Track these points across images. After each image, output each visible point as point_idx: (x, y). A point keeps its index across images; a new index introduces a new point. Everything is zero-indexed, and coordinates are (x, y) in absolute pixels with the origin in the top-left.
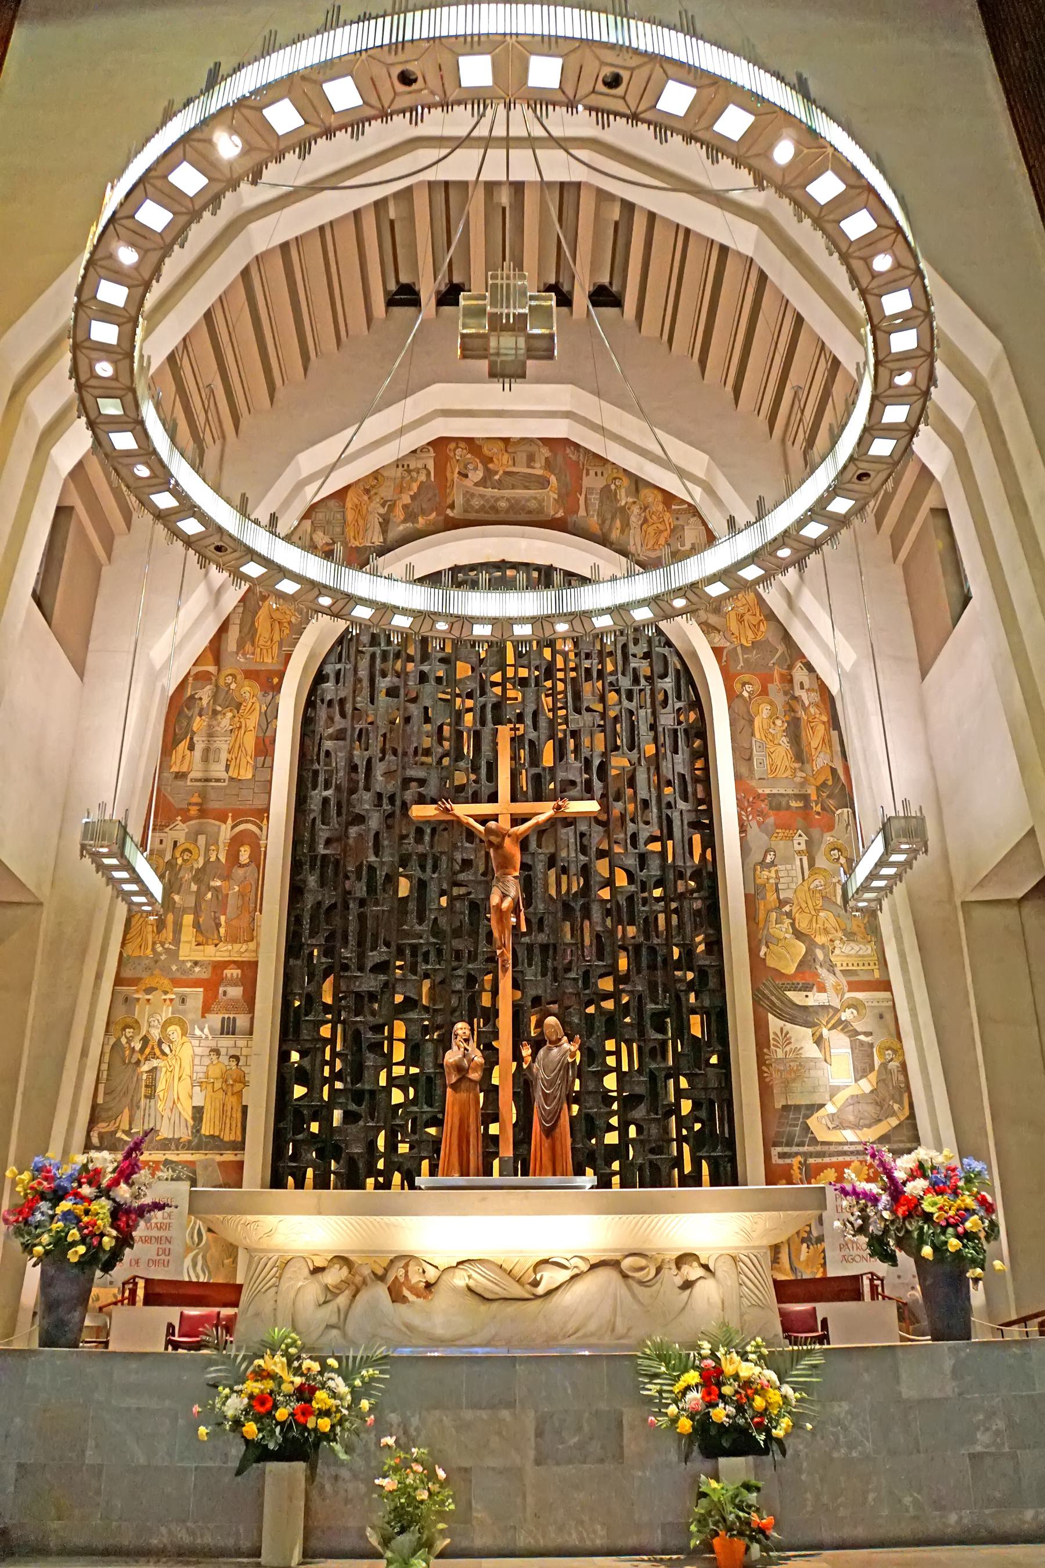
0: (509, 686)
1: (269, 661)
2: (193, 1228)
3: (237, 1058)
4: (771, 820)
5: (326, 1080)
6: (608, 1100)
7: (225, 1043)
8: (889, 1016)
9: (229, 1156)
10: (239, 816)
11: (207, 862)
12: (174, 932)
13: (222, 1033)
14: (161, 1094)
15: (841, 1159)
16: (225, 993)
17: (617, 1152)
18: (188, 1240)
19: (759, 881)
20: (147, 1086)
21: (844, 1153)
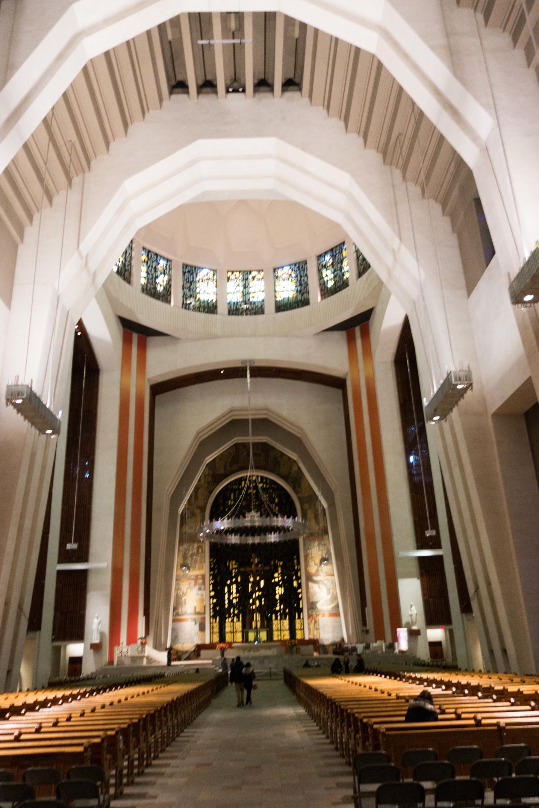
1: (201, 503)
6: (277, 600)
7: (200, 592)
9: (202, 616)
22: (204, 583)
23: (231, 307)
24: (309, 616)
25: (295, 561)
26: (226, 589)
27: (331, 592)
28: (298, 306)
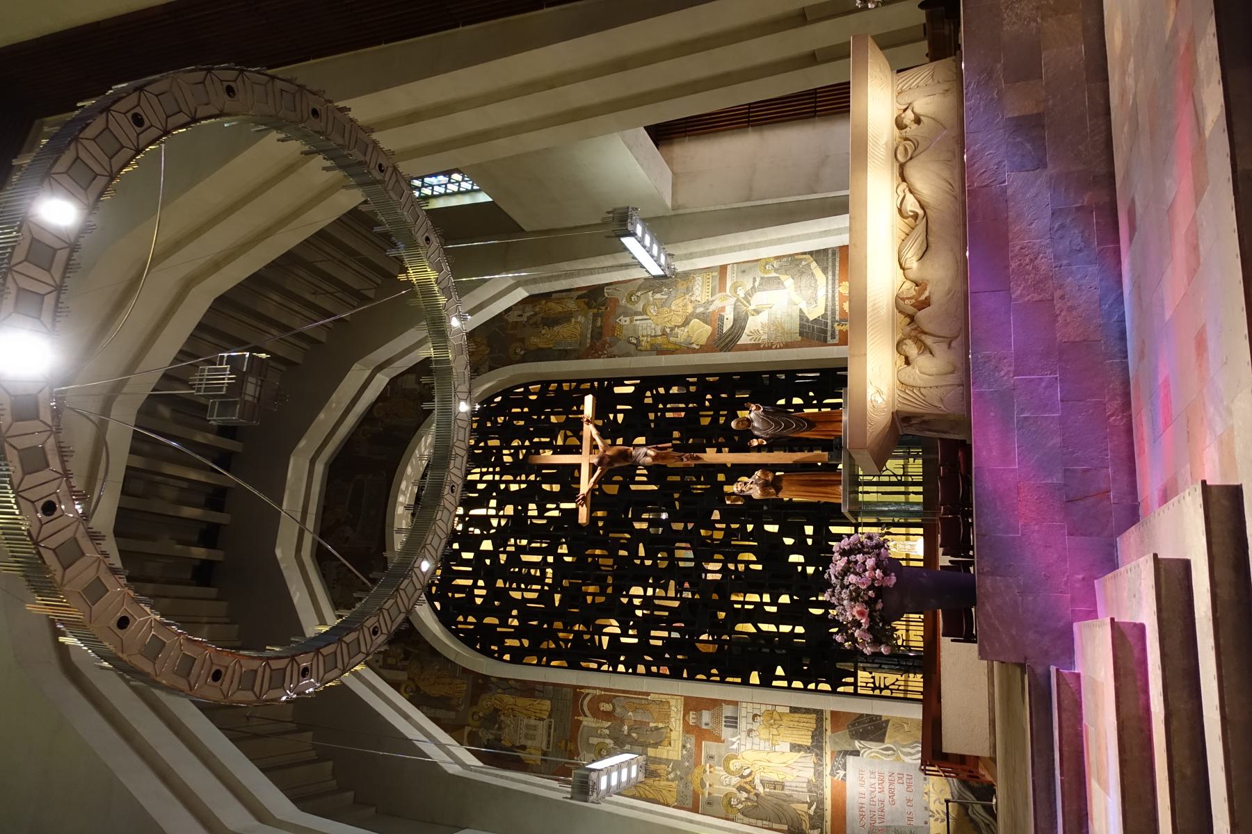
0: (501, 513)
1: (463, 686)
2: (882, 754)
3: (755, 716)
4: (608, 339)
5: (772, 651)
7: (743, 724)
8: (744, 267)
9: (828, 725)
10: (578, 710)
11: (609, 737)
12: (660, 763)
13: (736, 727)
14: (781, 777)
15: (837, 299)
16: (707, 724)
18: (891, 759)
19: (649, 348)
20: (775, 789)
21: (833, 296)
27: (774, 275)
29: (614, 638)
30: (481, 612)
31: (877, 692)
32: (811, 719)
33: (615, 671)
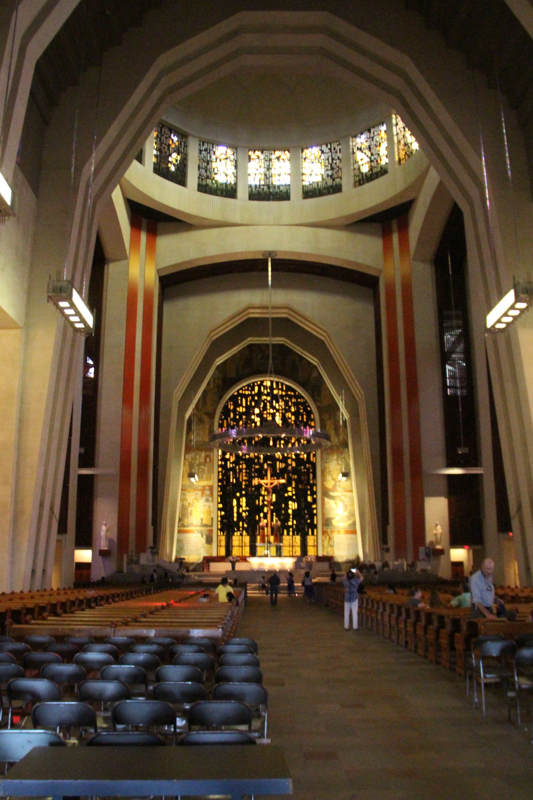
1: (210, 409)
6: (289, 515)
7: (207, 504)
9: (209, 528)
17: (292, 527)
22: (212, 494)
23: (252, 190)
24: (324, 533)
25: (311, 475)
26: (235, 502)
28: (329, 193)
29: (229, 460)
30: (234, 411)
31: (219, 541)
32: (210, 524)
33: (219, 460)
